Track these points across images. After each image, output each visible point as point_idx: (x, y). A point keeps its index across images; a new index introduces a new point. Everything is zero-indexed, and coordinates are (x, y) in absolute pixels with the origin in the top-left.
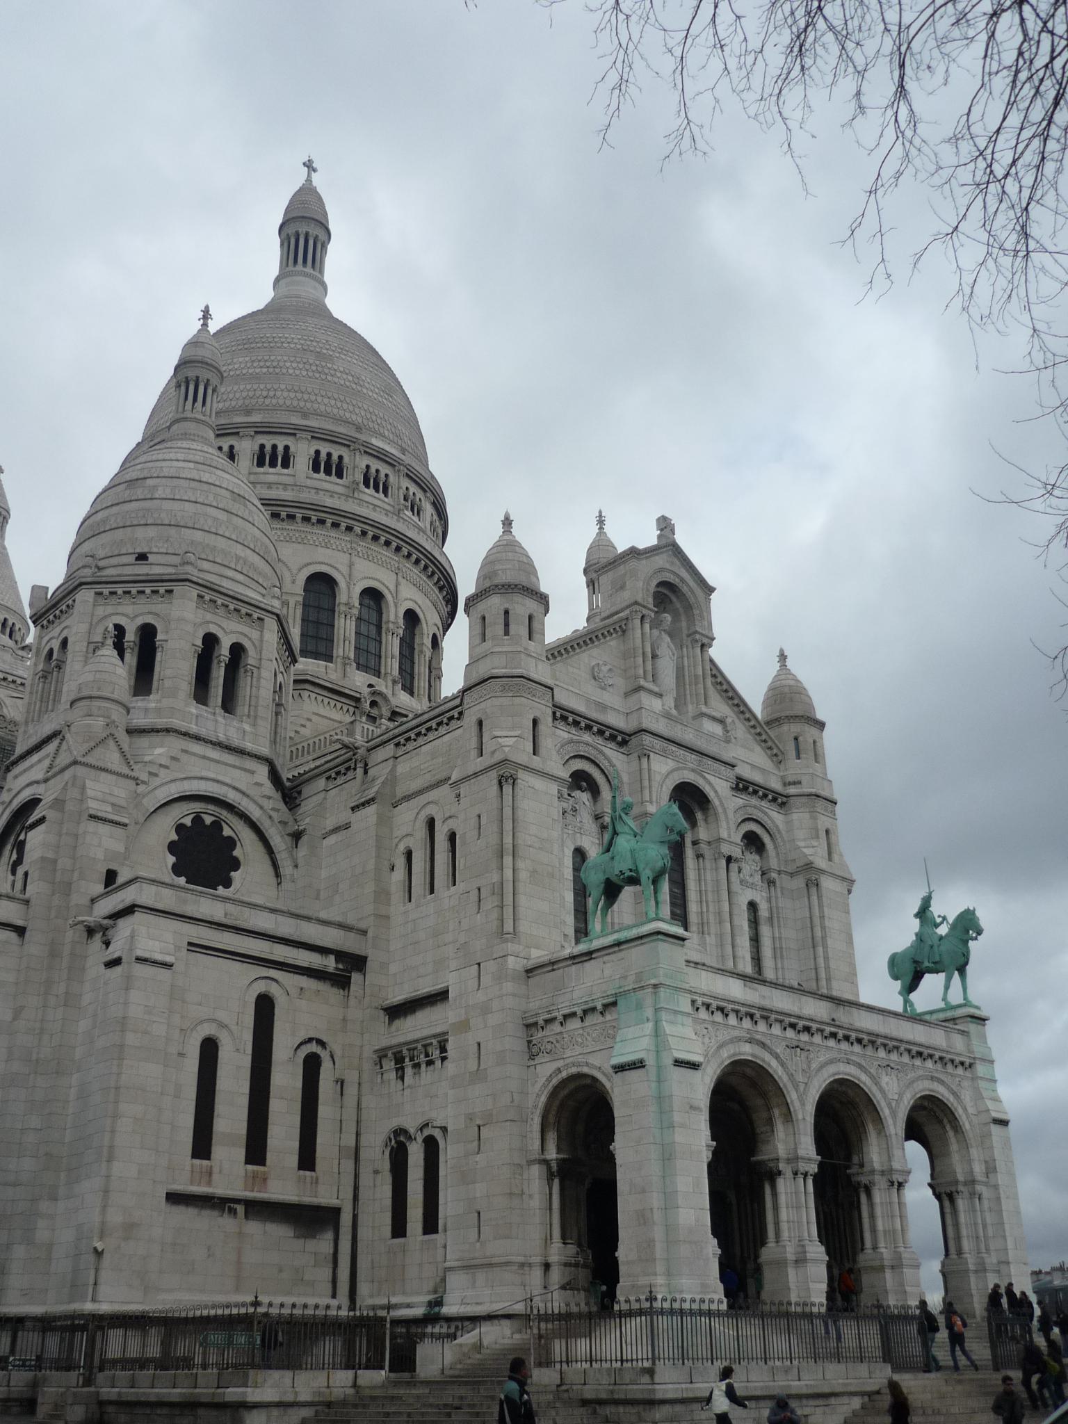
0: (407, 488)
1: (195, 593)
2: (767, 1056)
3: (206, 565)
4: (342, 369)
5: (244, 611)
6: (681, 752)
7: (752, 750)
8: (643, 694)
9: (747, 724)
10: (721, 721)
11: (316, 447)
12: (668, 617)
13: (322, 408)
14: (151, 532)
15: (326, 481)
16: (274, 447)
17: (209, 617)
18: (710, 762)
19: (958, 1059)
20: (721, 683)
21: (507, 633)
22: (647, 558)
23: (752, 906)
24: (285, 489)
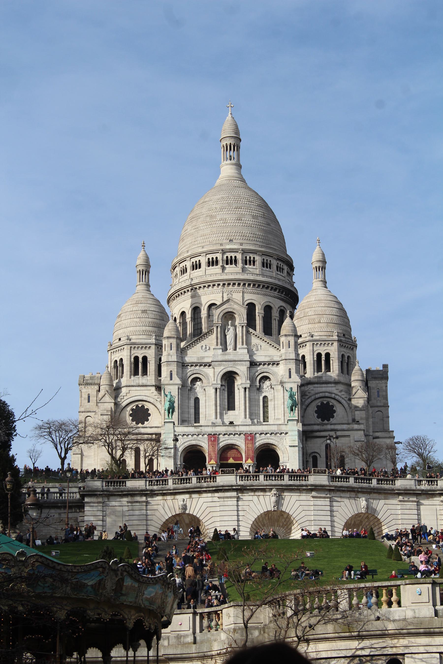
0: (246, 257)
1: (129, 347)
3: (134, 337)
4: (219, 219)
5: (144, 346)
6: (227, 363)
7: (268, 350)
9: (266, 343)
11: (208, 257)
13: (211, 239)
16: (196, 262)
17: (135, 351)
18: (239, 362)
19: (280, 432)
23: (265, 397)
24: (197, 279)
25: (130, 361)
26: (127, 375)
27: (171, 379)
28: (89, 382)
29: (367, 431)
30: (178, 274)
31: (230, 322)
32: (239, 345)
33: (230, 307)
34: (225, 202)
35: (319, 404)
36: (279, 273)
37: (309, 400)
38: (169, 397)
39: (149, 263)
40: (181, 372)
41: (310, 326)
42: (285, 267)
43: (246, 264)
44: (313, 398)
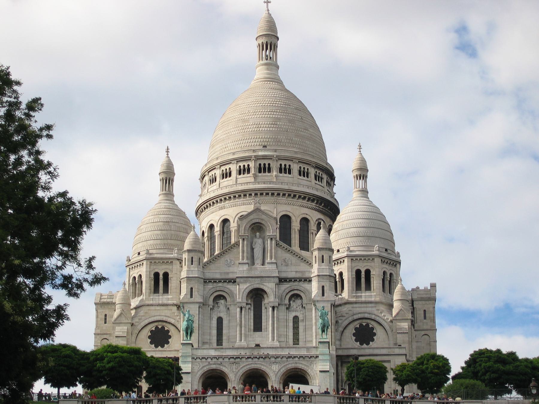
0: (281, 165)
2: (221, 367)
4: (251, 124)
5: (165, 262)
7: (299, 265)
8: (240, 265)
9: (297, 257)
10: (276, 263)
12: (258, 234)
14: (140, 245)
15: (243, 178)
16: (226, 169)
17: (155, 267)
20: (284, 247)
21: (185, 265)
22: (245, 218)
24: (226, 188)
25: (150, 278)
26: (146, 293)
27: (191, 296)
28: (105, 300)
29: (410, 356)
30: (207, 184)
31: (258, 234)
32: (268, 260)
33: (257, 217)
34: (259, 105)
35: (358, 326)
36: (317, 182)
37: (347, 322)
38: (187, 316)
39: (174, 171)
40: (203, 289)
41: (349, 240)
42: (325, 177)
43: (281, 172)
44: (351, 319)
